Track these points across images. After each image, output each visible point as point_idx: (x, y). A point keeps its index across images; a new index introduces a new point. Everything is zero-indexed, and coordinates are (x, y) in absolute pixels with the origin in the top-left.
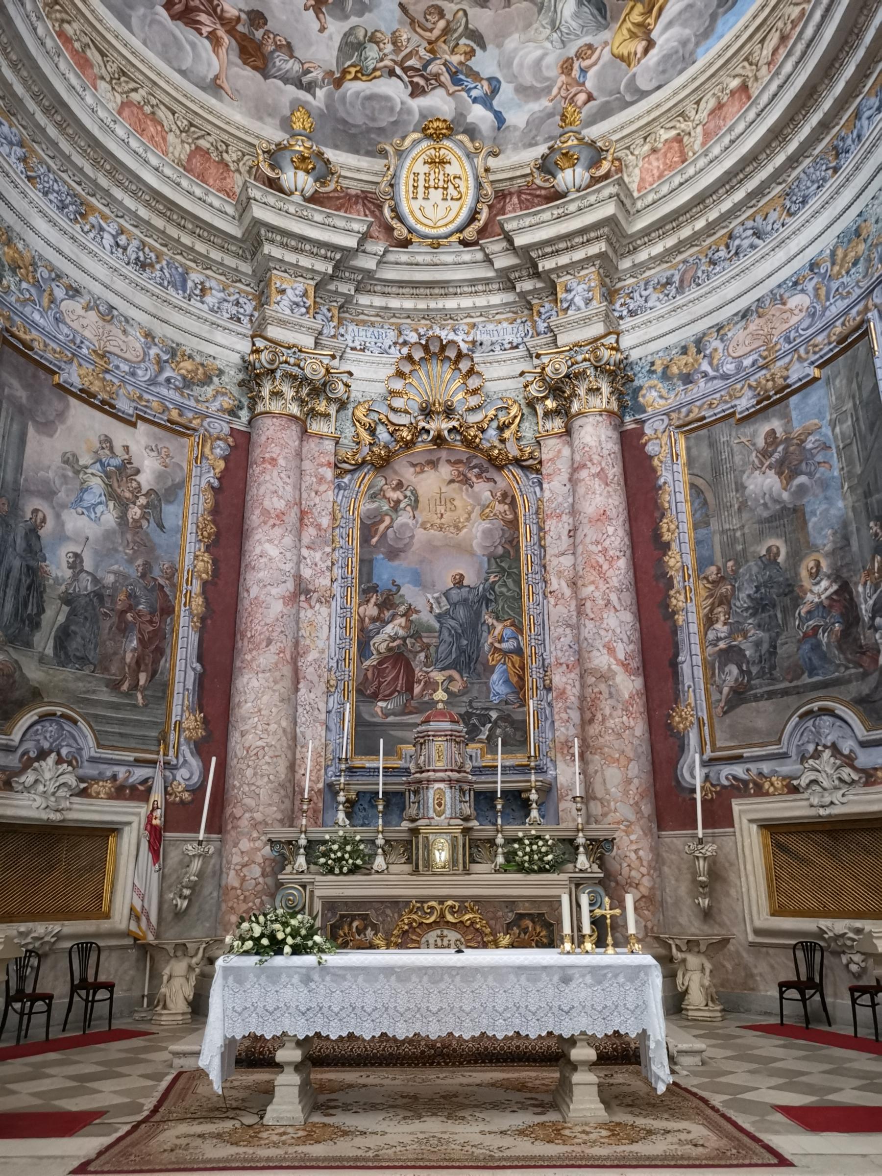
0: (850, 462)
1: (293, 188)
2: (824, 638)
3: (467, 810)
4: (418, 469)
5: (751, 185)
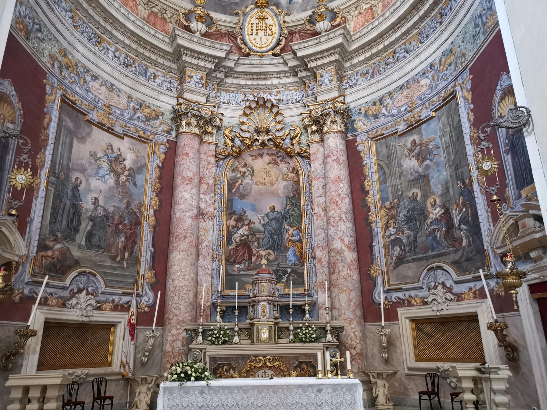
0: (449, 154)
1: (196, 30)
3: (276, 314)
4: (254, 158)
5: (404, 29)
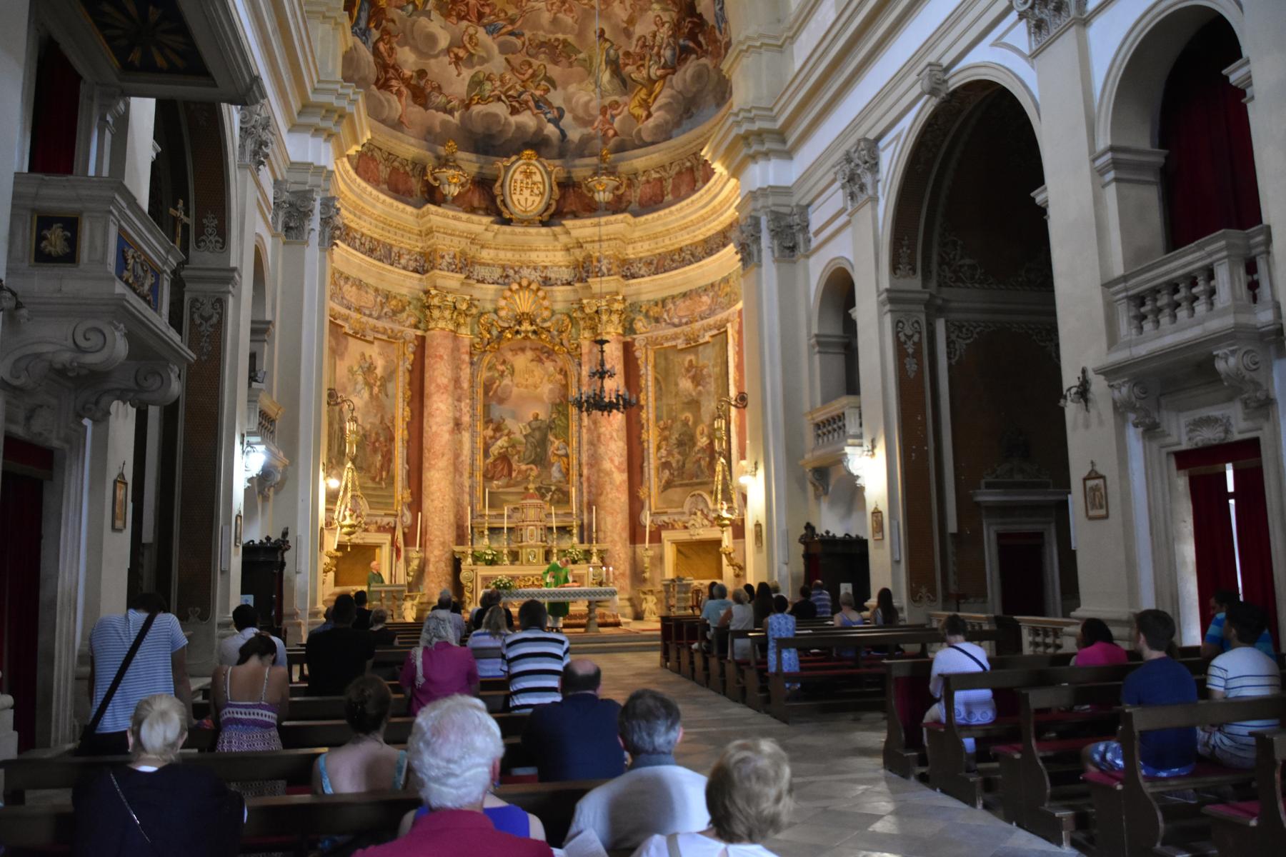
2: (703, 463)
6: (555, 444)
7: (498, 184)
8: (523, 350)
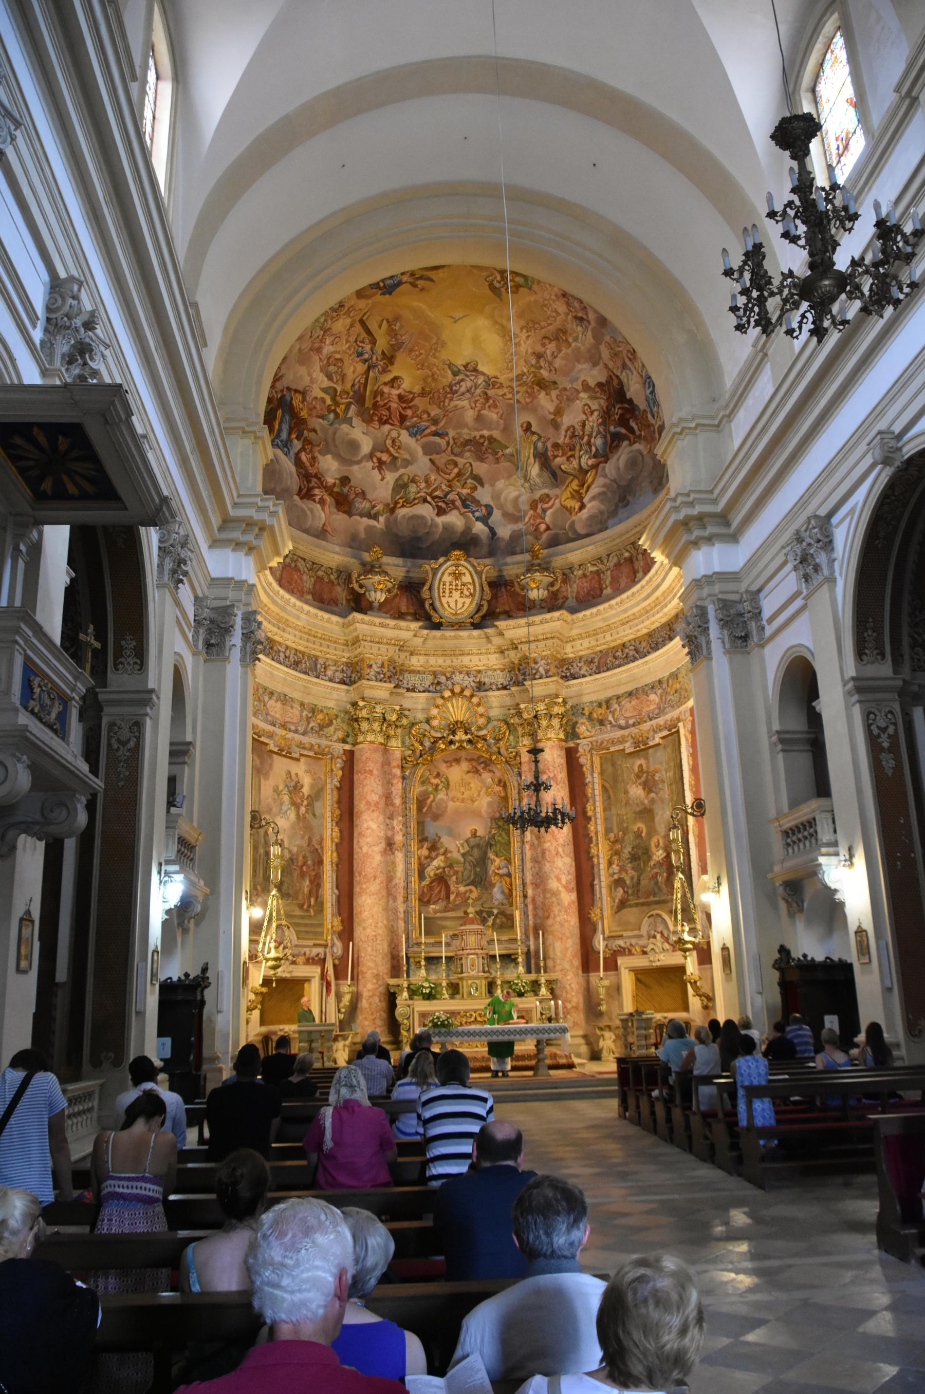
2: (660, 879)
6: (496, 863)
7: (426, 588)
8: (458, 761)
